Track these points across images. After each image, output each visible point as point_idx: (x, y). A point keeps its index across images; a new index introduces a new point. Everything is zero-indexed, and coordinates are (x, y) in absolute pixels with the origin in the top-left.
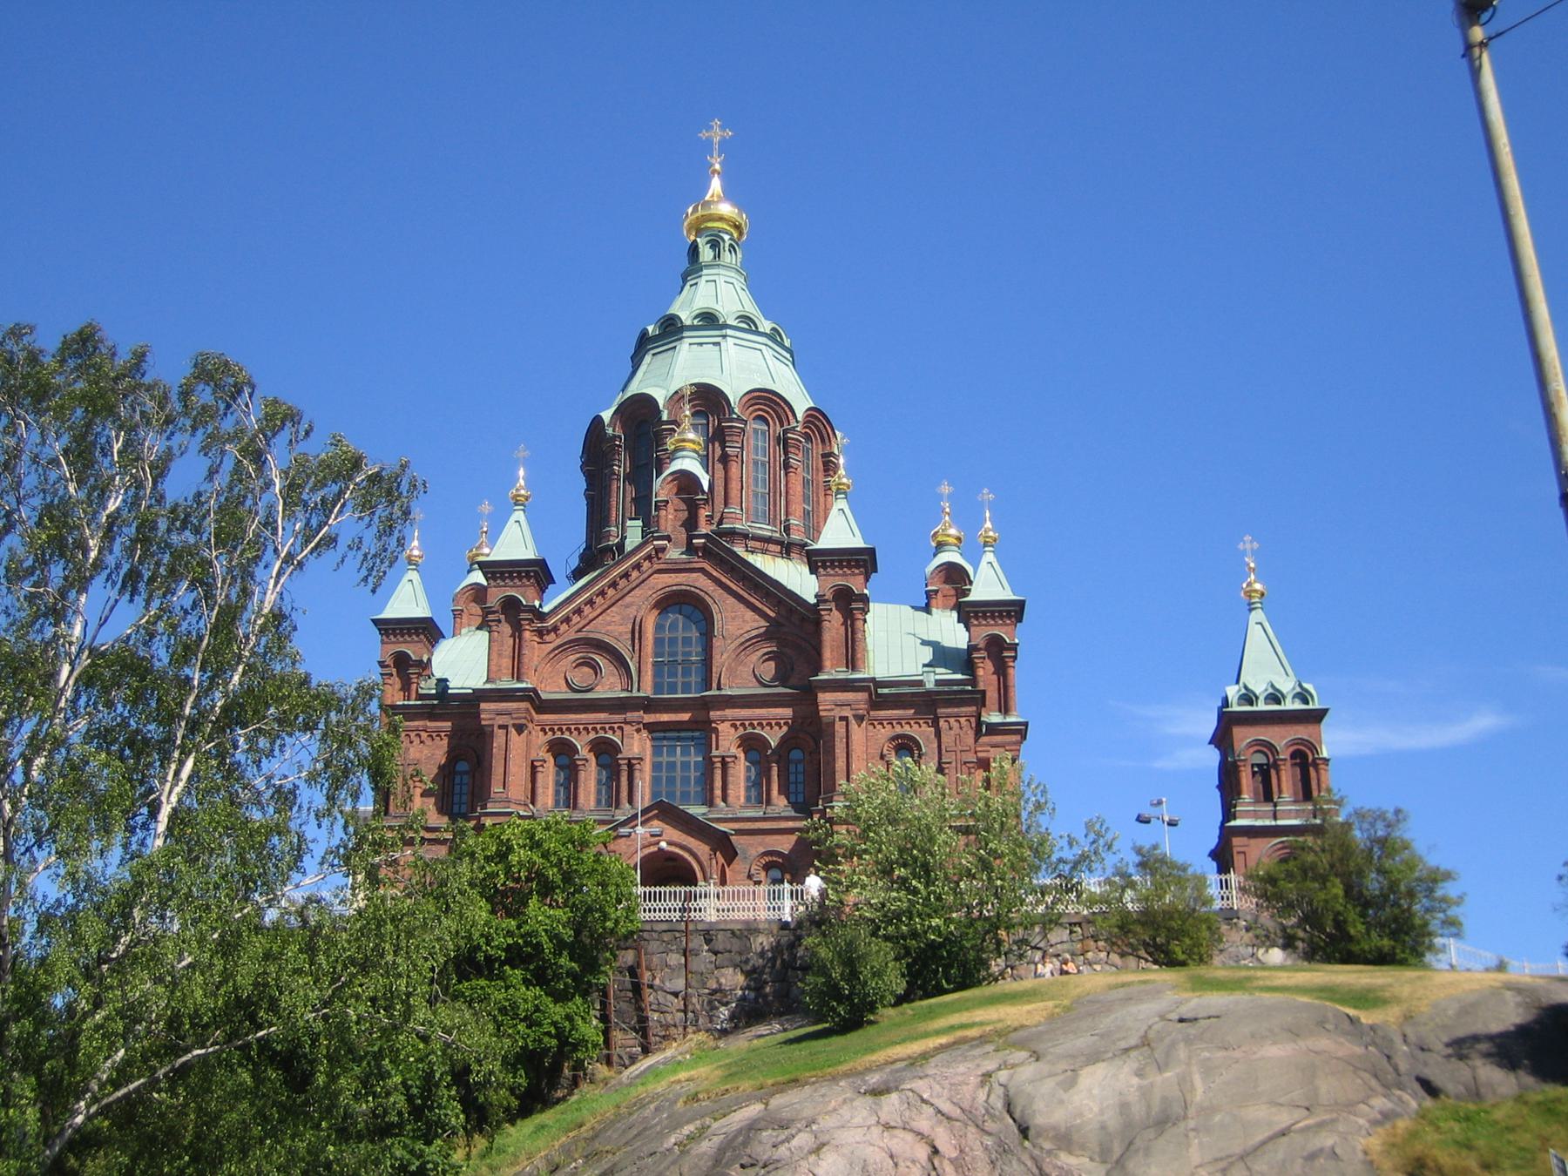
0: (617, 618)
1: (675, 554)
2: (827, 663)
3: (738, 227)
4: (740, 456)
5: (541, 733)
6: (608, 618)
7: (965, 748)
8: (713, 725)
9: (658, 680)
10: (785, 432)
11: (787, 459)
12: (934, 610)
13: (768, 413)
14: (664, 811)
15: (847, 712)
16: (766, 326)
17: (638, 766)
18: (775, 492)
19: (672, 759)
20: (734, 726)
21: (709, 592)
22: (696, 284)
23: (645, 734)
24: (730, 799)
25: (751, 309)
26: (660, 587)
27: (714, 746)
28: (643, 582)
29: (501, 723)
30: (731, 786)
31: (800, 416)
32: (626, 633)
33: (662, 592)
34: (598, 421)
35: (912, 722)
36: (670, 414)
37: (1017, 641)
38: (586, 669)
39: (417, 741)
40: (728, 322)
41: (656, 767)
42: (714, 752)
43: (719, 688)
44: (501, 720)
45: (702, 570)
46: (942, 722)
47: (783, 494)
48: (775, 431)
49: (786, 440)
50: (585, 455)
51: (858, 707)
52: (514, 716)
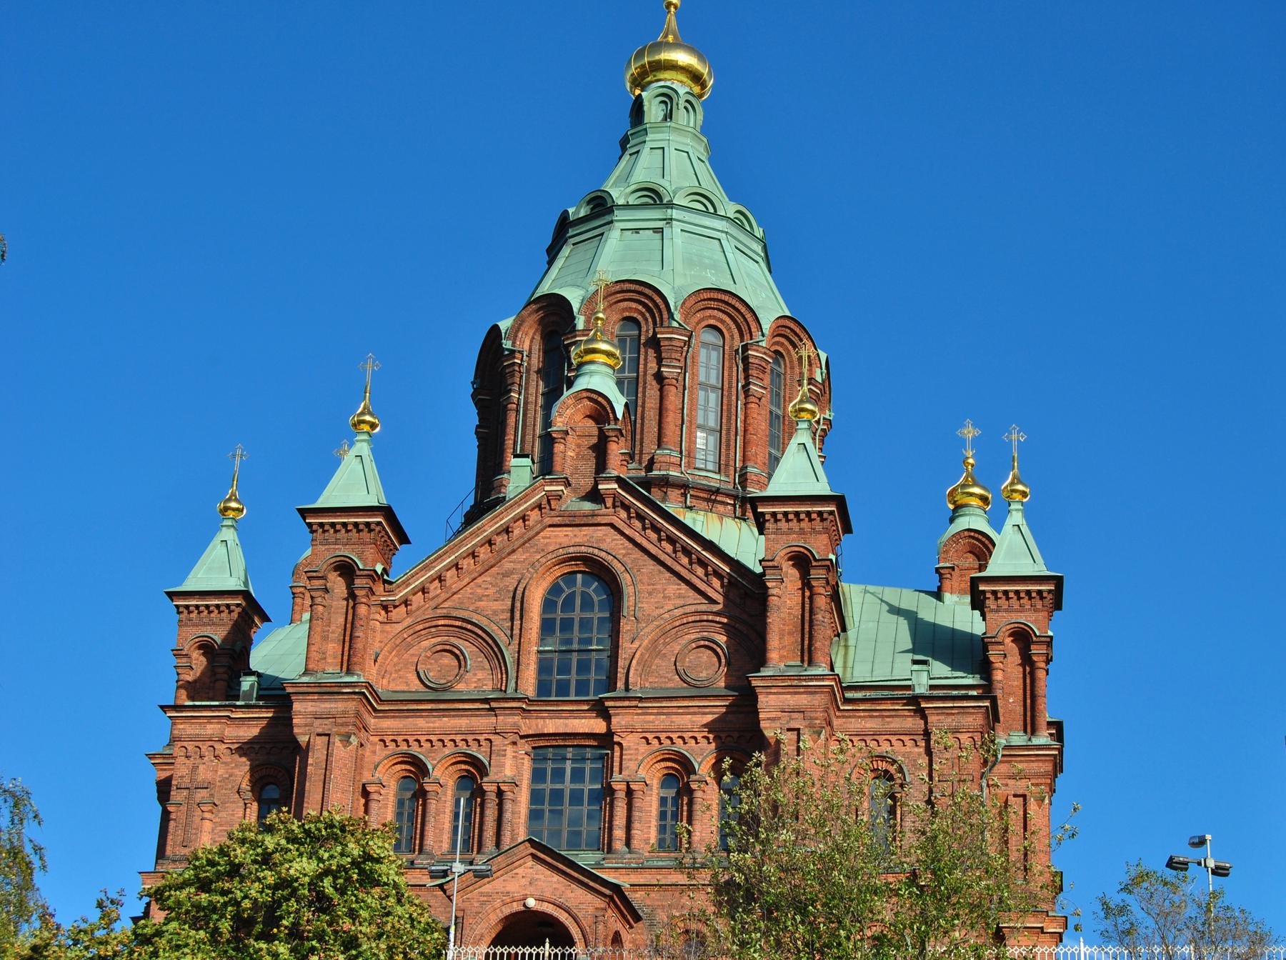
0: (491, 591)
1: (572, 503)
2: (773, 655)
3: (696, 78)
4: (680, 378)
5: (379, 746)
6: (479, 591)
9: (544, 677)
10: (745, 348)
11: (747, 384)
12: (947, 596)
13: (722, 321)
14: (545, 853)
16: (730, 209)
17: (509, 795)
18: (728, 430)
19: (558, 786)
21: (620, 557)
22: (638, 152)
25: (710, 183)
26: (551, 548)
27: (616, 769)
28: (530, 539)
29: (320, 731)
30: (636, 825)
31: (768, 326)
32: (503, 611)
33: (549, 557)
34: (495, 330)
35: (893, 739)
37: (1050, 633)
39: (209, 756)
41: (536, 797)
43: (627, 689)
44: (320, 726)
45: (612, 526)
47: (740, 432)
48: (731, 347)
49: (745, 359)
50: (478, 380)
51: (813, 715)
52: (339, 721)
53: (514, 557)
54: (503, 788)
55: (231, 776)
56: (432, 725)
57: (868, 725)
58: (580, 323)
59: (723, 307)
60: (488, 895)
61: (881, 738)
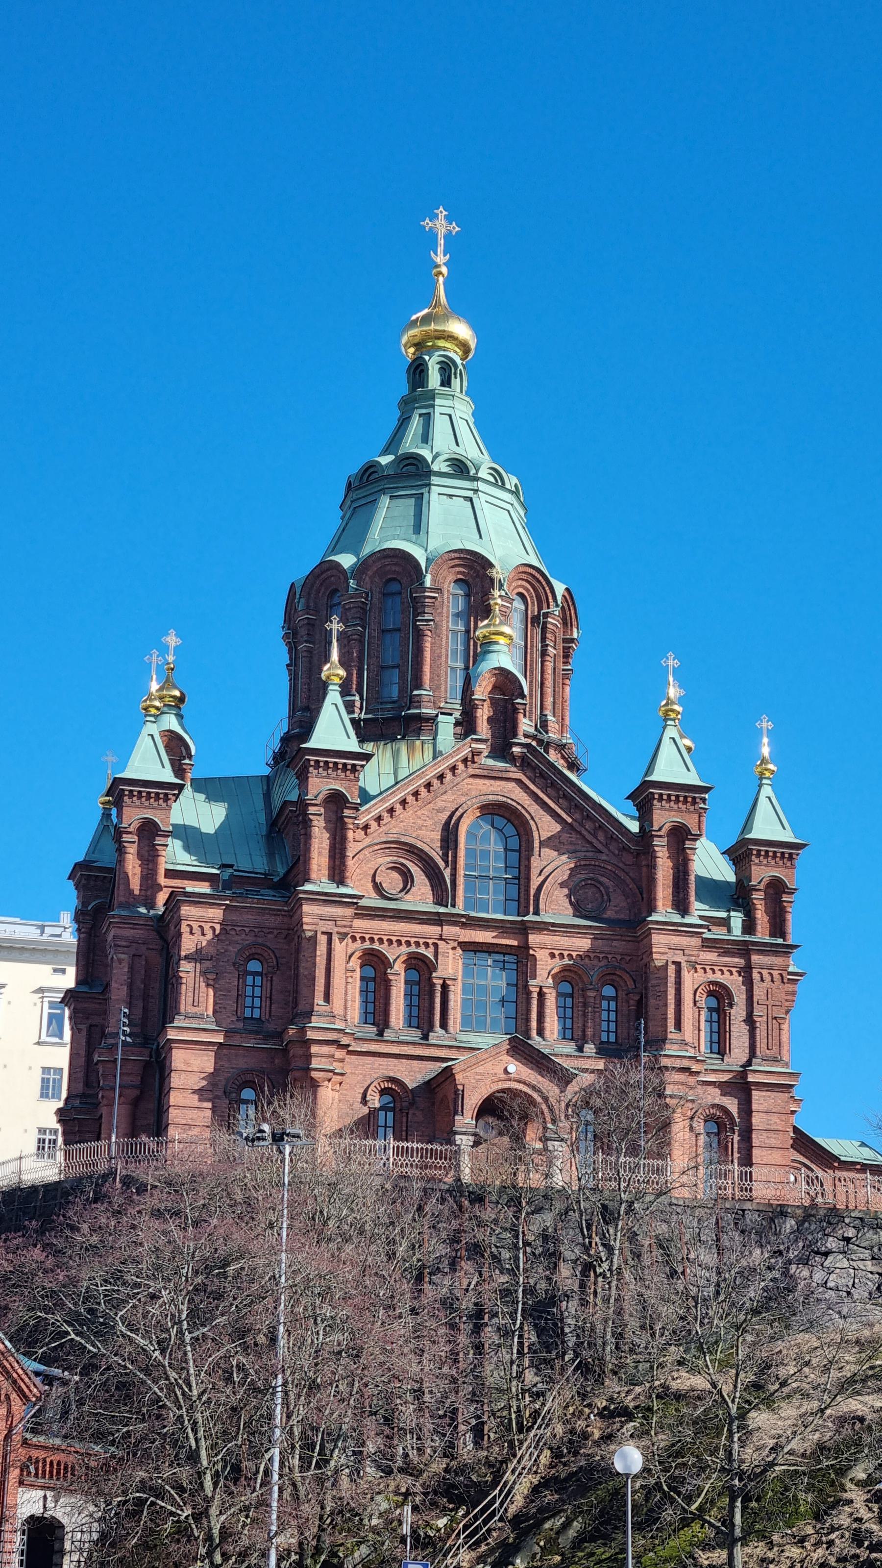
0: (430, 822)
2: (660, 903)
7: (777, 1003)
8: (531, 952)
15: (679, 958)
17: (452, 988)
20: (553, 956)
21: (526, 806)
23: (459, 951)
24: (547, 1033)
26: (474, 793)
29: (324, 930)
35: (725, 969)
36: (434, 580)
38: (395, 875)
40: (479, 475)
42: (532, 982)
46: (756, 976)
51: (691, 953)
53: (444, 797)
54: (448, 982)
55: (226, 951)
56: (392, 927)
57: (708, 958)
58: (428, 582)
59: (530, 579)
60: (481, 1074)
61: (716, 968)
